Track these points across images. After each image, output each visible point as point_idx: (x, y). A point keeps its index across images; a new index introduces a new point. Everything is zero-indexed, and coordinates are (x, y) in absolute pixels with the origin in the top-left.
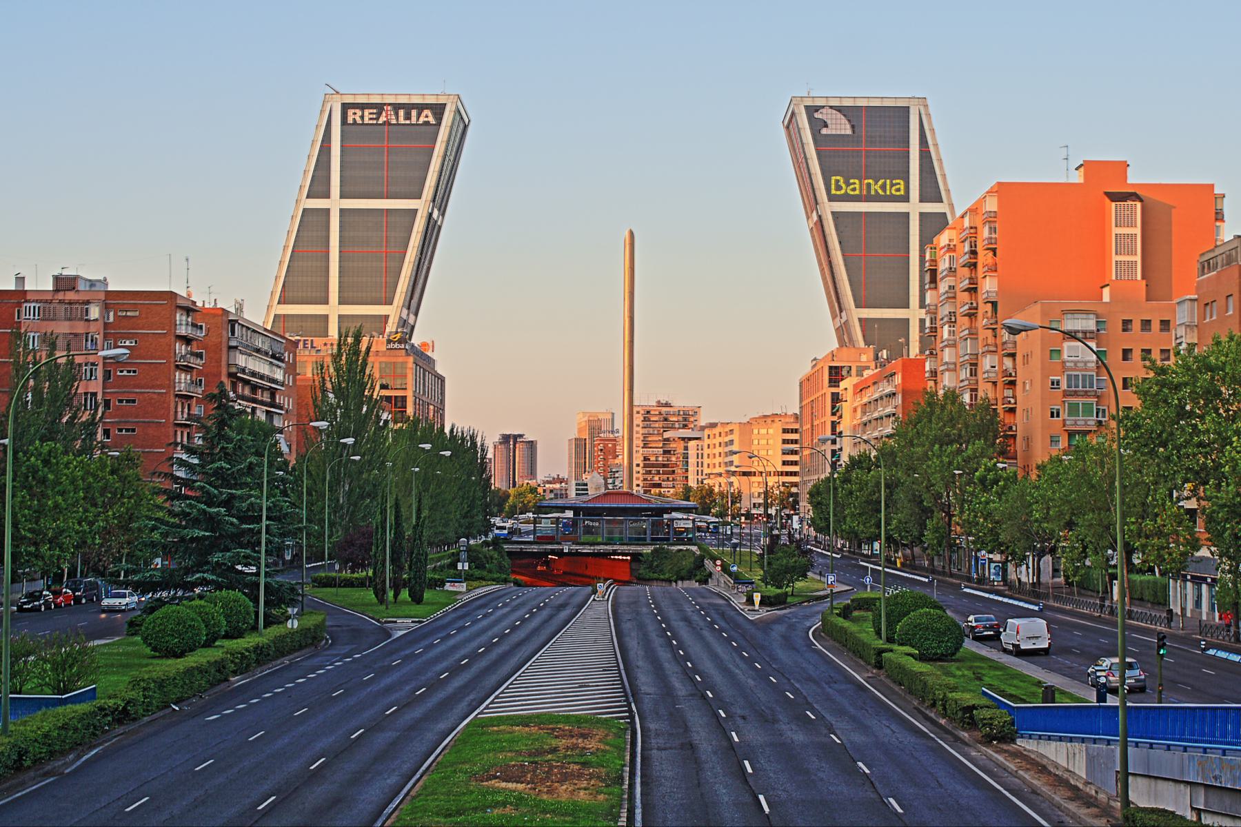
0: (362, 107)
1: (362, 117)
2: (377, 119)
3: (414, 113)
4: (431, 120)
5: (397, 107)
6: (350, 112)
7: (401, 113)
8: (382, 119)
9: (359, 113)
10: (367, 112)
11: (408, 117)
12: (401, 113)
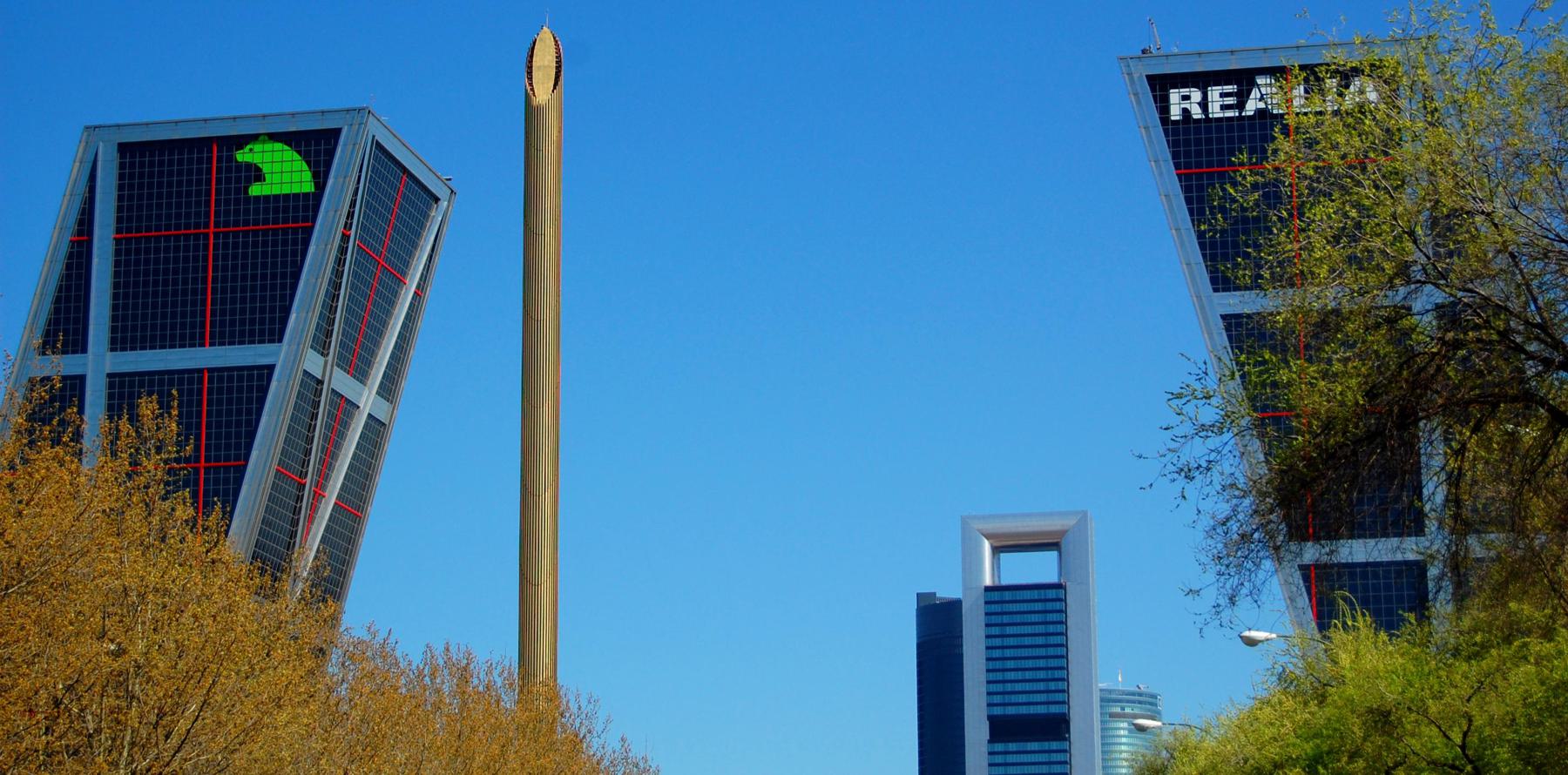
0: (1203, 80)
1: (1204, 105)
2: (1241, 106)
3: (1331, 83)
6: (1175, 96)
8: (1251, 106)
9: (1196, 96)
10: (1214, 93)
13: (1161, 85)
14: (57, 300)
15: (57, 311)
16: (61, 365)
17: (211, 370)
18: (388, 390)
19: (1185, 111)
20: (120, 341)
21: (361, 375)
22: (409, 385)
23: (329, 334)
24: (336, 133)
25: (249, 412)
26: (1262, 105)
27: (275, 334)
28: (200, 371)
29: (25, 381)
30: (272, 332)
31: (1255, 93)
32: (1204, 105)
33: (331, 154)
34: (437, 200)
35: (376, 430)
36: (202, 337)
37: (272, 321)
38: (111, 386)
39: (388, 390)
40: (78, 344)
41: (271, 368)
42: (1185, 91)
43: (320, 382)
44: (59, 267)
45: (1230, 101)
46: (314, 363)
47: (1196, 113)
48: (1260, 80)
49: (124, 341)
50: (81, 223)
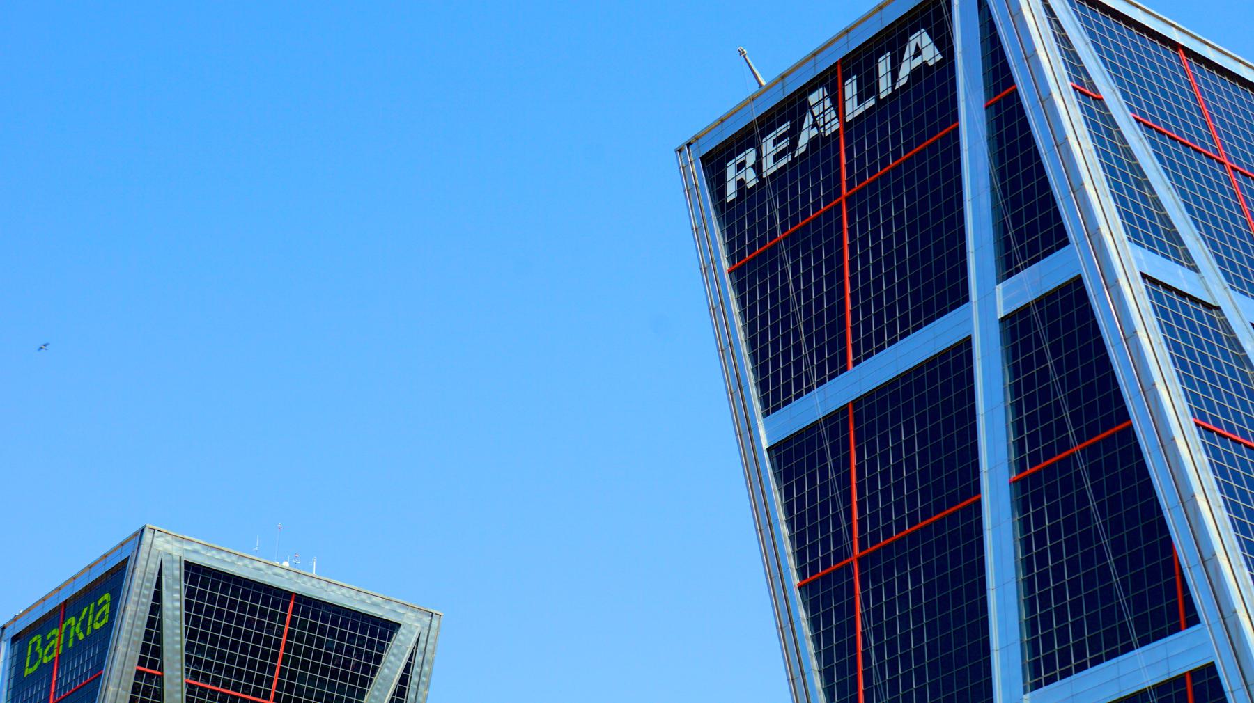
1: (758, 167)
2: (793, 146)
3: (884, 65)
4: (931, 55)
5: (830, 80)
6: (731, 171)
7: (851, 88)
8: (803, 140)
11: (868, 88)
12: (851, 88)
13: (714, 163)
19: (741, 183)
26: (814, 132)
31: (808, 120)
32: (758, 167)
42: (740, 158)
45: (784, 144)
47: (750, 178)
48: (813, 98)
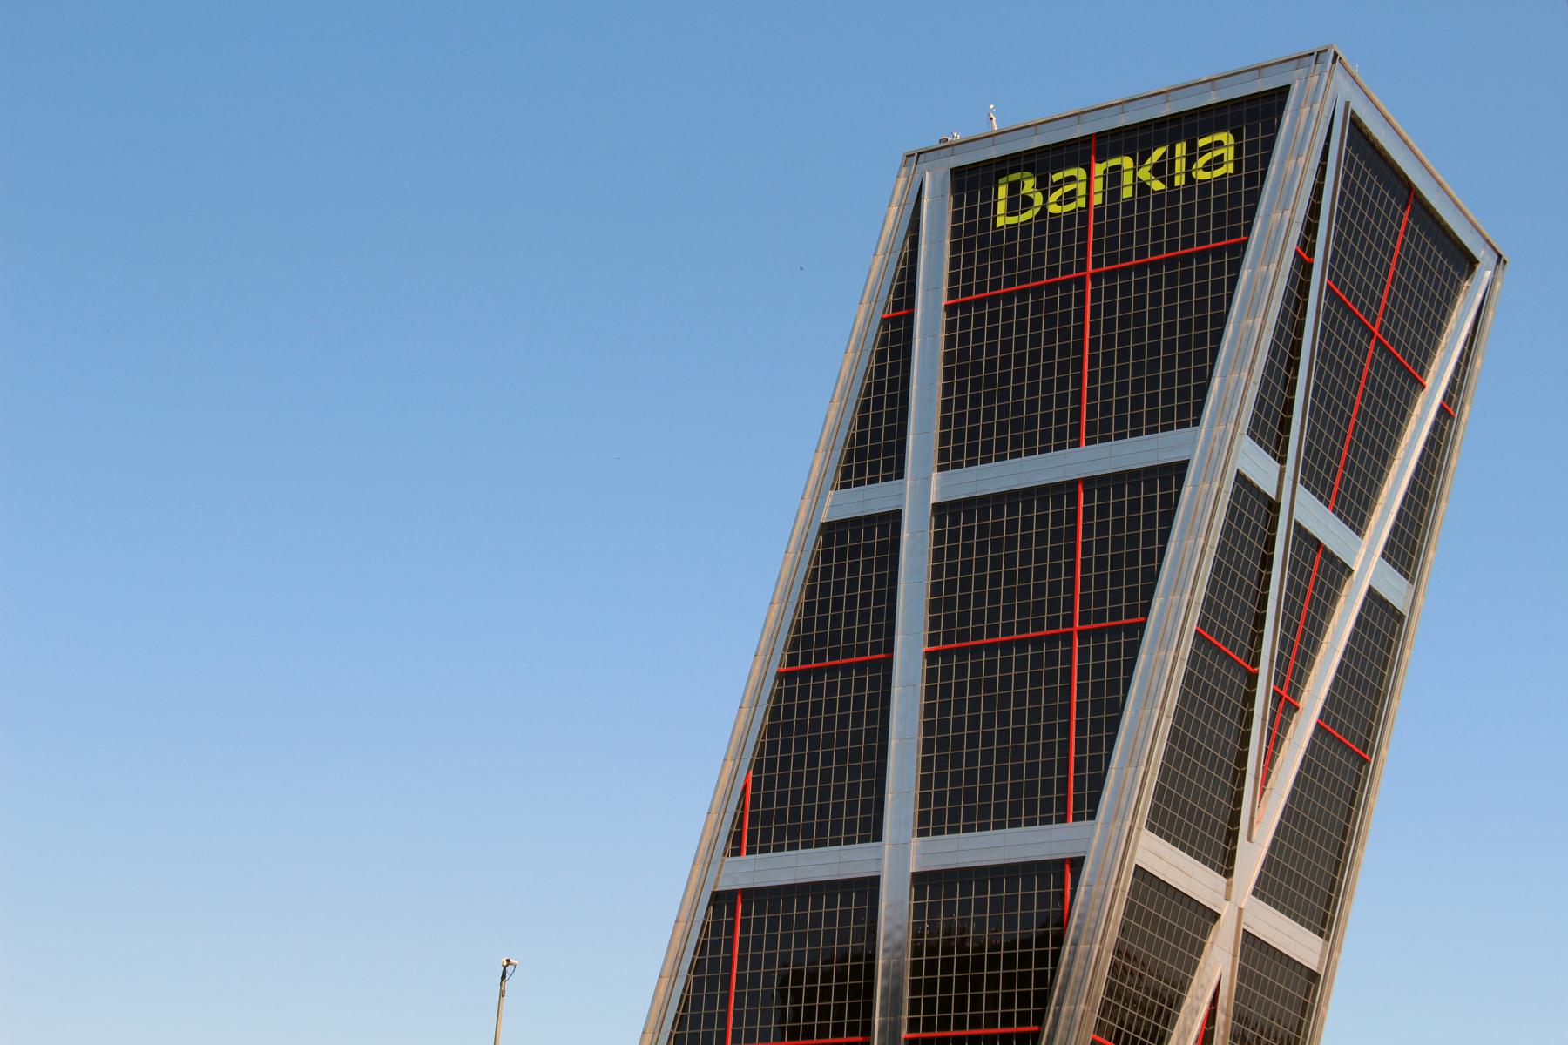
14: (864, 406)
15: (863, 422)
16: (870, 499)
17: (1088, 482)
18: (1404, 550)
20: (952, 455)
21: (1356, 519)
22: (1436, 555)
23: (1285, 426)
24: (1284, 91)
25: (1149, 538)
27: (1187, 410)
28: (1073, 484)
29: (815, 529)
30: (1183, 411)
33: (1272, 130)
34: (1472, 262)
35: (1382, 625)
36: (1076, 431)
37: (1184, 394)
38: (939, 522)
39: (1404, 550)
40: (895, 469)
41: (1182, 466)
43: (1274, 506)
44: (867, 359)
46: (1262, 470)
49: (958, 453)
50: (899, 291)
